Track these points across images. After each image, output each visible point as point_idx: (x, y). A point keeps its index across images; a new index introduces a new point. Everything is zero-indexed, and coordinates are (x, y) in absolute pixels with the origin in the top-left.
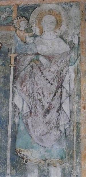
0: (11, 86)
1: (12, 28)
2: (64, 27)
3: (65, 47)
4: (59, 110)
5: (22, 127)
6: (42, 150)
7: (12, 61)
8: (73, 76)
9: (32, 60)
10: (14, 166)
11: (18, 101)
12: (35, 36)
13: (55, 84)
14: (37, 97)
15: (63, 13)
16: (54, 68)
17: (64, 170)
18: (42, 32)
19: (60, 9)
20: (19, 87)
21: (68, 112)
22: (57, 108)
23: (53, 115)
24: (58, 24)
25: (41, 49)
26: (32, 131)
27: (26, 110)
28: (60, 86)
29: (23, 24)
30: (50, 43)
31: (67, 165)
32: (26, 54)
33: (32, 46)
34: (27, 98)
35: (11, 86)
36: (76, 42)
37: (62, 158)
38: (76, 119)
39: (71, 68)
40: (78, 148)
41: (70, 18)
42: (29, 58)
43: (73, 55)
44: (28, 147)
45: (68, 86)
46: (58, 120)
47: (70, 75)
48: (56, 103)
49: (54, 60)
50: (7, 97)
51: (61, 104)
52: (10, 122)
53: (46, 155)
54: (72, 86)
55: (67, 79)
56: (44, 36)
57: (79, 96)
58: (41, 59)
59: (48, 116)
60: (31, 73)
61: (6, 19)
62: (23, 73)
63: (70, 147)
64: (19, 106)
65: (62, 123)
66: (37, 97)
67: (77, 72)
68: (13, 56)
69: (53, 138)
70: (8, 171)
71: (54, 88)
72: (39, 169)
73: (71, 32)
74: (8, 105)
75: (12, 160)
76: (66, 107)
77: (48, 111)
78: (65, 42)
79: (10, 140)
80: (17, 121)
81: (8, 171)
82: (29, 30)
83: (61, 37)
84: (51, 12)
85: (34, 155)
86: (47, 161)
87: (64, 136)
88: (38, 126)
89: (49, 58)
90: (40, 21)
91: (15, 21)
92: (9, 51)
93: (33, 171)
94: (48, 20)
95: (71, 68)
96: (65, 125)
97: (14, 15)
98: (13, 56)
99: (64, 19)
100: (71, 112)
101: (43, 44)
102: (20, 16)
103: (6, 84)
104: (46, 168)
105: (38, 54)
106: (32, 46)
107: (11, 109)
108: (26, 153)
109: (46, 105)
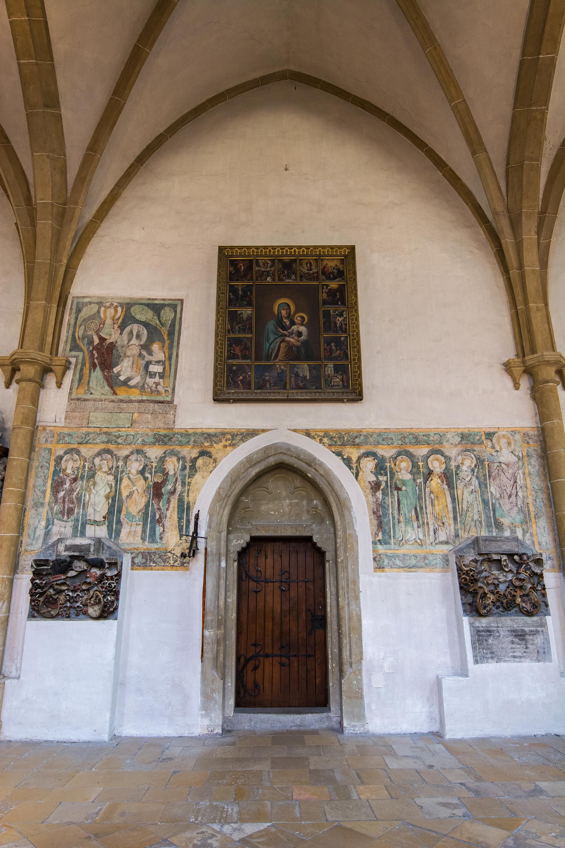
0: (488, 481)
1: (483, 446)
2: (513, 447)
3: (516, 459)
4: (516, 496)
5: (497, 505)
6: (510, 518)
7: (487, 467)
8: (522, 476)
9: (498, 466)
10: (497, 527)
11: (493, 489)
12: (497, 451)
13: (512, 481)
14: (503, 488)
15: (511, 438)
16: (511, 471)
17: (523, 529)
18: (501, 449)
19: (509, 435)
20: (492, 482)
21: (521, 497)
22: (515, 495)
23: (513, 498)
24: (509, 444)
25: (502, 459)
26: (503, 507)
27: (498, 495)
28: (515, 482)
29: (489, 443)
30: (506, 456)
31: (525, 527)
32: (494, 463)
33: (496, 457)
34: (498, 489)
35: (488, 481)
36: (521, 455)
37: (522, 523)
38: (526, 501)
39: (520, 471)
40: (530, 517)
41: (516, 441)
42: (496, 465)
43: (520, 463)
44: (502, 516)
45: (520, 482)
46: (517, 501)
47: (520, 476)
48: (514, 492)
49: (510, 466)
50: (486, 487)
51: (517, 492)
52: (490, 502)
53: (513, 521)
54: (522, 482)
55: (518, 478)
56: (502, 451)
57: (527, 488)
58: (503, 465)
59: (511, 499)
60: (498, 474)
61: (479, 440)
62: (494, 474)
63: (525, 517)
64: (494, 493)
65: (519, 503)
66: (503, 488)
67: (524, 474)
68: (486, 463)
69: (515, 512)
70: (494, 530)
71: (512, 483)
72: (510, 528)
73: (517, 449)
74: (488, 492)
75: (495, 524)
76: (520, 494)
77: (510, 496)
78: (515, 455)
79: (492, 513)
80: (494, 501)
81: (494, 530)
82: (493, 447)
83: (512, 452)
84: (504, 436)
85: (506, 521)
86: (514, 525)
87: (521, 510)
88: (506, 505)
89: (507, 465)
90: (499, 442)
91: (484, 442)
92: (484, 460)
93: (507, 530)
94: (503, 441)
95: (520, 471)
96: (521, 504)
97: (483, 437)
98: (486, 463)
99: (512, 441)
100: (523, 497)
101: (503, 456)
102: (487, 439)
103: (485, 480)
104: (514, 528)
105: (500, 463)
106: (496, 457)
107: (489, 494)
108: (502, 520)
109: (509, 493)
